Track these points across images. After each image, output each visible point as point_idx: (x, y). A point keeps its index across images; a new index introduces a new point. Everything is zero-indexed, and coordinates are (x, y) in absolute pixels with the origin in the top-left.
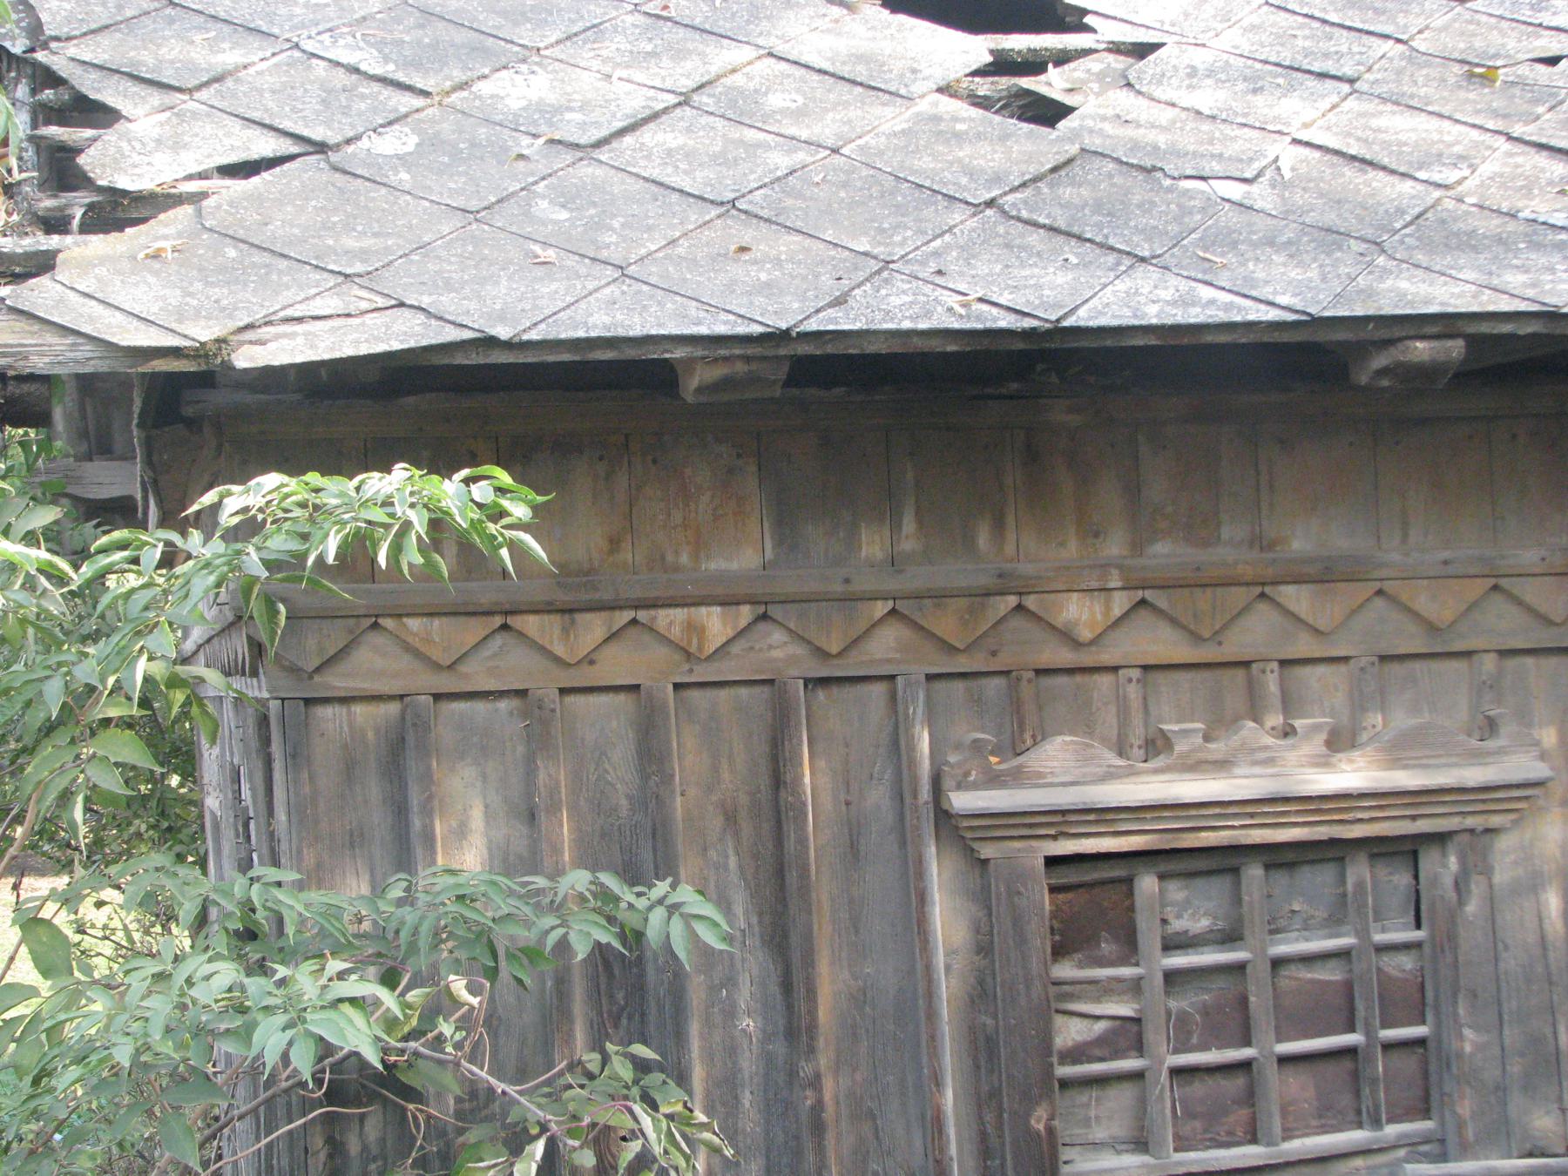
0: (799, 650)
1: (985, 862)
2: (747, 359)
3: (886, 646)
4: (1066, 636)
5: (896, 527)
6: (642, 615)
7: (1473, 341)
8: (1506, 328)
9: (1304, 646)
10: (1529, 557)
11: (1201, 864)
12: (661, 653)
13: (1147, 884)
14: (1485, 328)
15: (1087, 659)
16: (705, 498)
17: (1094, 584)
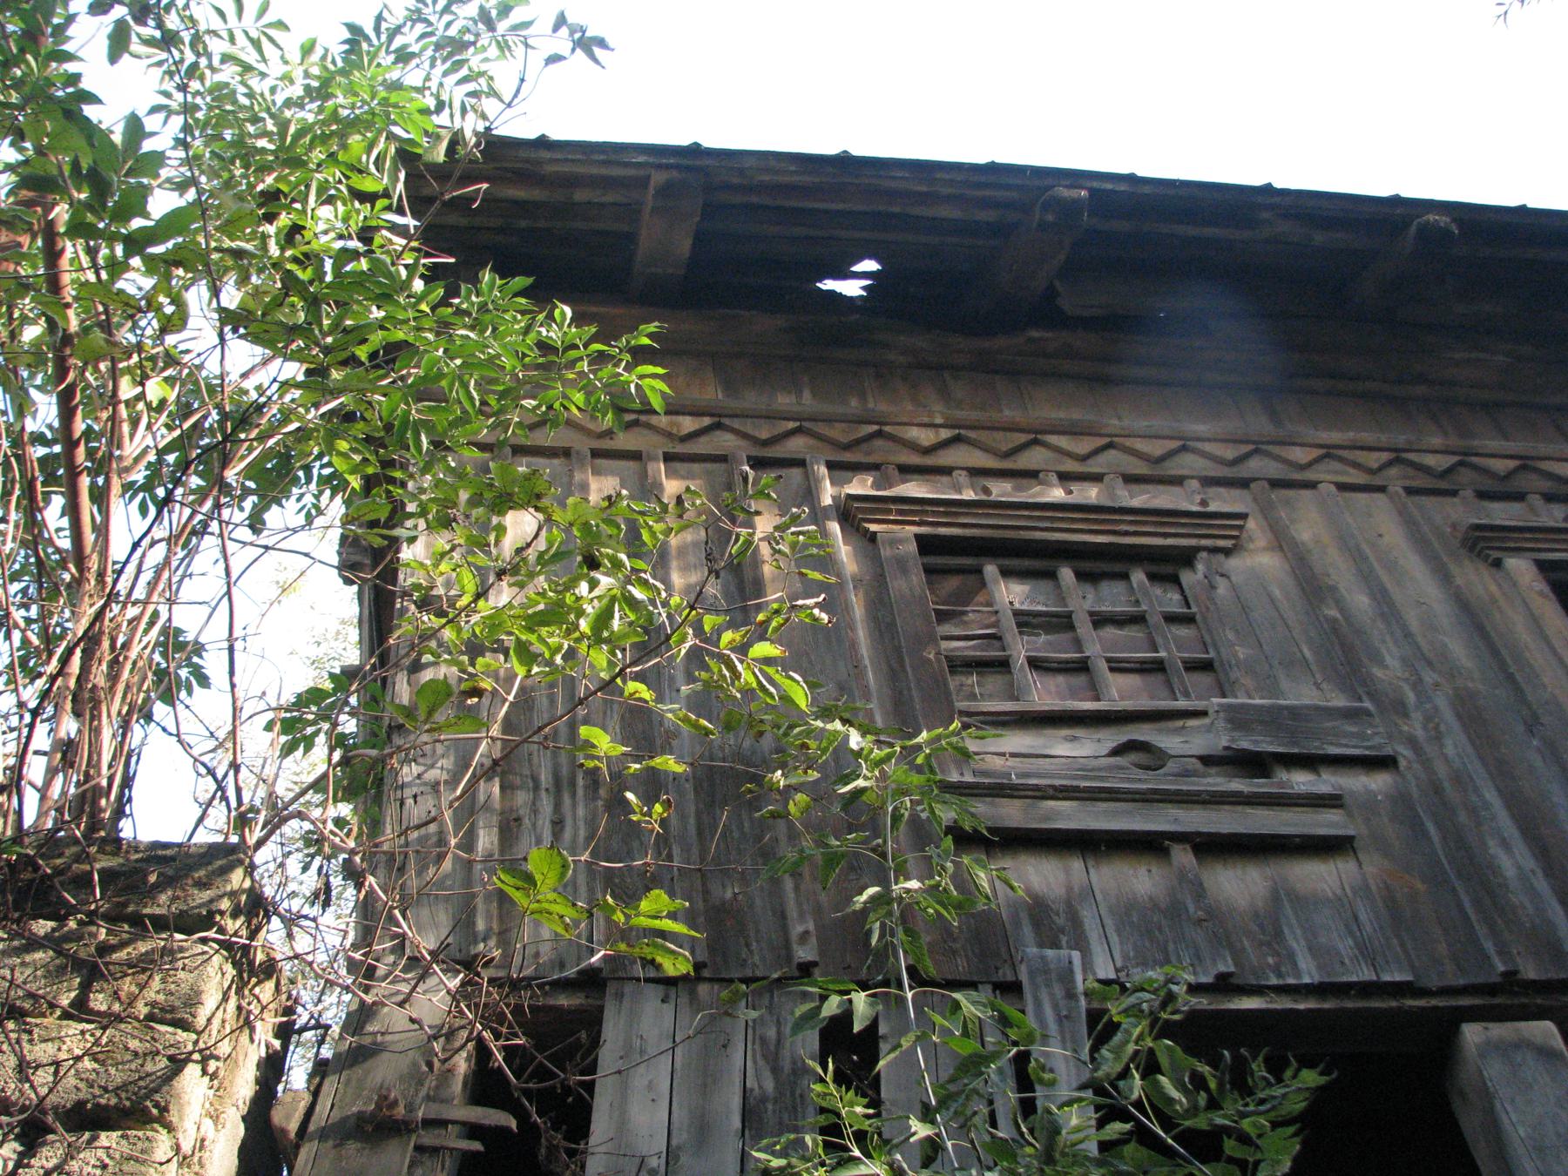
0: (742, 443)
1: (873, 537)
2: (677, 167)
3: (796, 446)
4: (914, 446)
5: (799, 394)
6: (643, 418)
7: (1090, 190)
8: (1109, 186)
9: (1071, 466)
10: (1201, 428)
11: (1026, 563)
12: (656, 438)
13: (991, 570)
14: (1095, 184)
15: (929, 461)
16: (681, 379)
17: (926, 420)
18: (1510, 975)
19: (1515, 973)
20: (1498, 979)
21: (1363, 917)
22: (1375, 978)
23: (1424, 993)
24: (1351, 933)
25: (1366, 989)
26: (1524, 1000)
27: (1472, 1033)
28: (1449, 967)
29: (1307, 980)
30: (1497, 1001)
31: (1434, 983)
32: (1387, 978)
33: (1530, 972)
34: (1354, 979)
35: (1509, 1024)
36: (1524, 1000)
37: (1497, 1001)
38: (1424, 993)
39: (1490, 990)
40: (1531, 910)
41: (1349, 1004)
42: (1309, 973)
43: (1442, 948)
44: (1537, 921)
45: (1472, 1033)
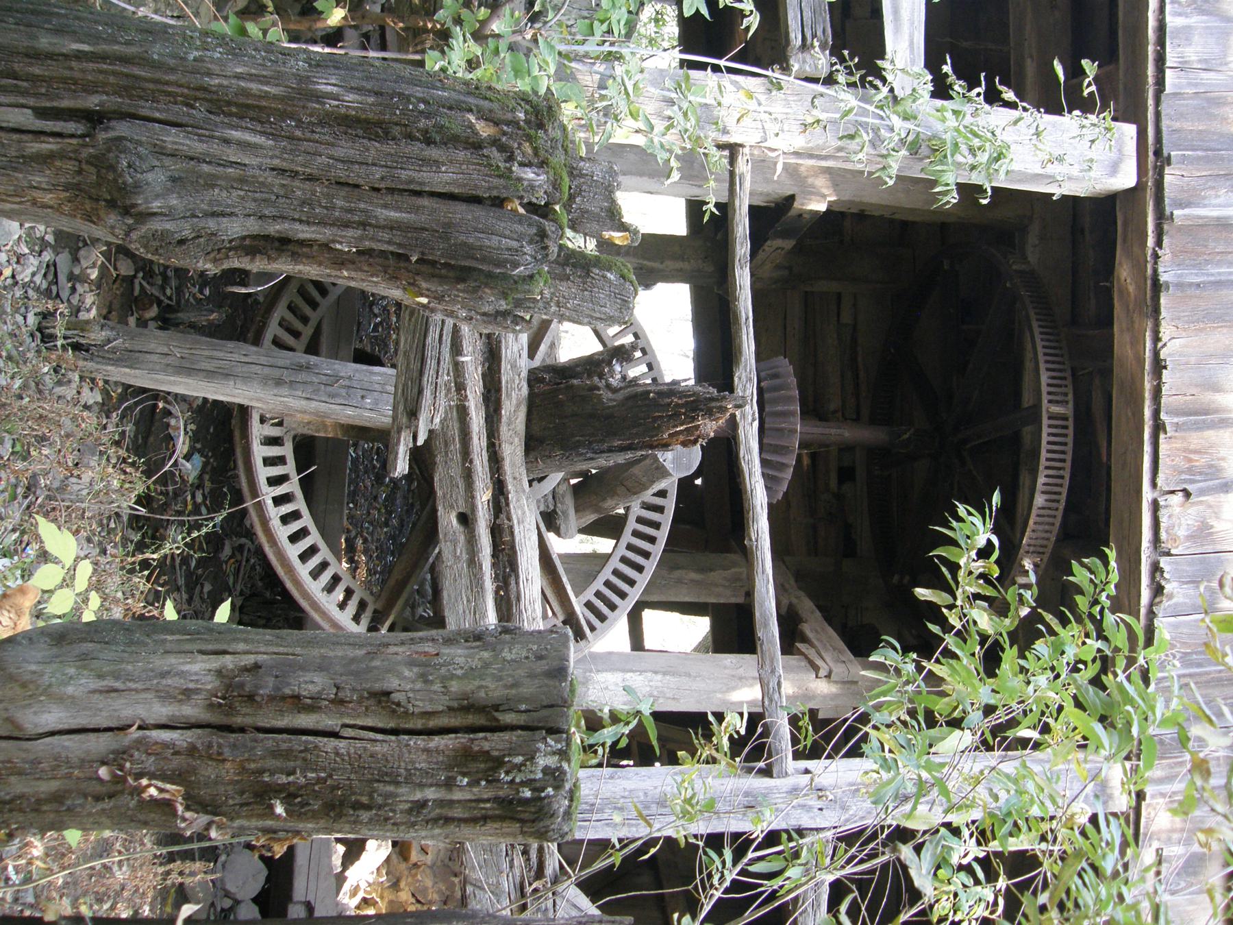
18: (1168, 161)
19: (1169, 164)
20: (1165, 153)
21: (1211, 75)
22: (1168, 64)
23: (1158, 102)
24: (1200, 61)
25: (1161, 59)
26: (1150, 173)
27: (1130, 130)
28: (1177, 125)
29: (1168, 19)
30: (1151, 154)
31: (1164, 108)
32: (1168, 73)
33: (1170, 177)
34: (1168, 50)
35: (1135, 154)
36: (1150, 173)
37: (1151, 154)
38: (1158, 102)
39: (1158, 153)
40: (1214, 202)
41: (1151, 48)
42: (1171, 21)
43: (1188, 126)
44: (1206, 202)
45: (1130, 130)
